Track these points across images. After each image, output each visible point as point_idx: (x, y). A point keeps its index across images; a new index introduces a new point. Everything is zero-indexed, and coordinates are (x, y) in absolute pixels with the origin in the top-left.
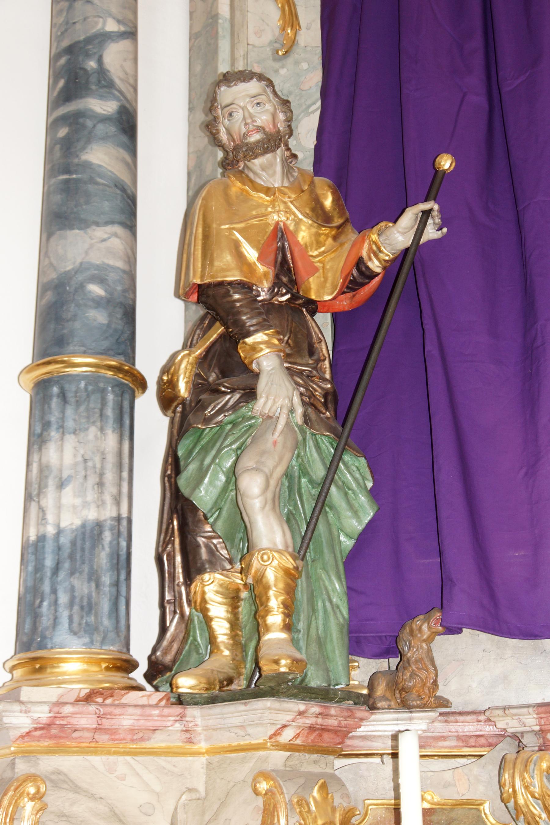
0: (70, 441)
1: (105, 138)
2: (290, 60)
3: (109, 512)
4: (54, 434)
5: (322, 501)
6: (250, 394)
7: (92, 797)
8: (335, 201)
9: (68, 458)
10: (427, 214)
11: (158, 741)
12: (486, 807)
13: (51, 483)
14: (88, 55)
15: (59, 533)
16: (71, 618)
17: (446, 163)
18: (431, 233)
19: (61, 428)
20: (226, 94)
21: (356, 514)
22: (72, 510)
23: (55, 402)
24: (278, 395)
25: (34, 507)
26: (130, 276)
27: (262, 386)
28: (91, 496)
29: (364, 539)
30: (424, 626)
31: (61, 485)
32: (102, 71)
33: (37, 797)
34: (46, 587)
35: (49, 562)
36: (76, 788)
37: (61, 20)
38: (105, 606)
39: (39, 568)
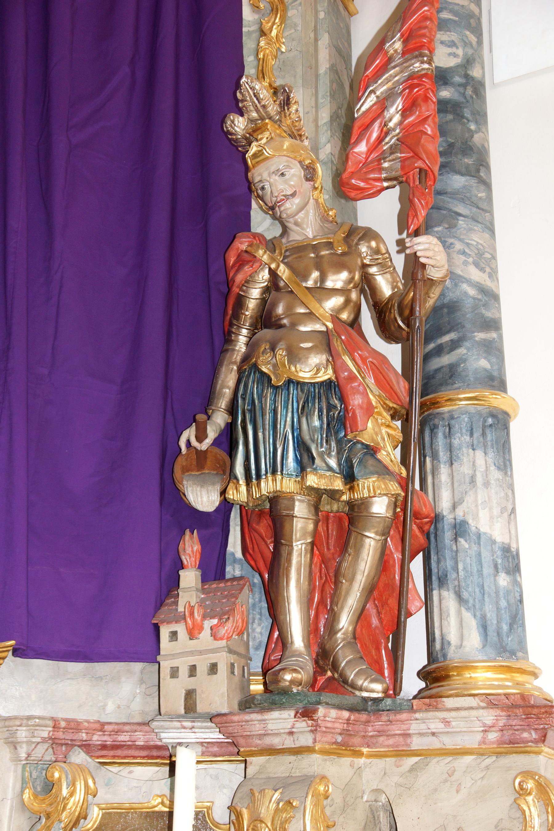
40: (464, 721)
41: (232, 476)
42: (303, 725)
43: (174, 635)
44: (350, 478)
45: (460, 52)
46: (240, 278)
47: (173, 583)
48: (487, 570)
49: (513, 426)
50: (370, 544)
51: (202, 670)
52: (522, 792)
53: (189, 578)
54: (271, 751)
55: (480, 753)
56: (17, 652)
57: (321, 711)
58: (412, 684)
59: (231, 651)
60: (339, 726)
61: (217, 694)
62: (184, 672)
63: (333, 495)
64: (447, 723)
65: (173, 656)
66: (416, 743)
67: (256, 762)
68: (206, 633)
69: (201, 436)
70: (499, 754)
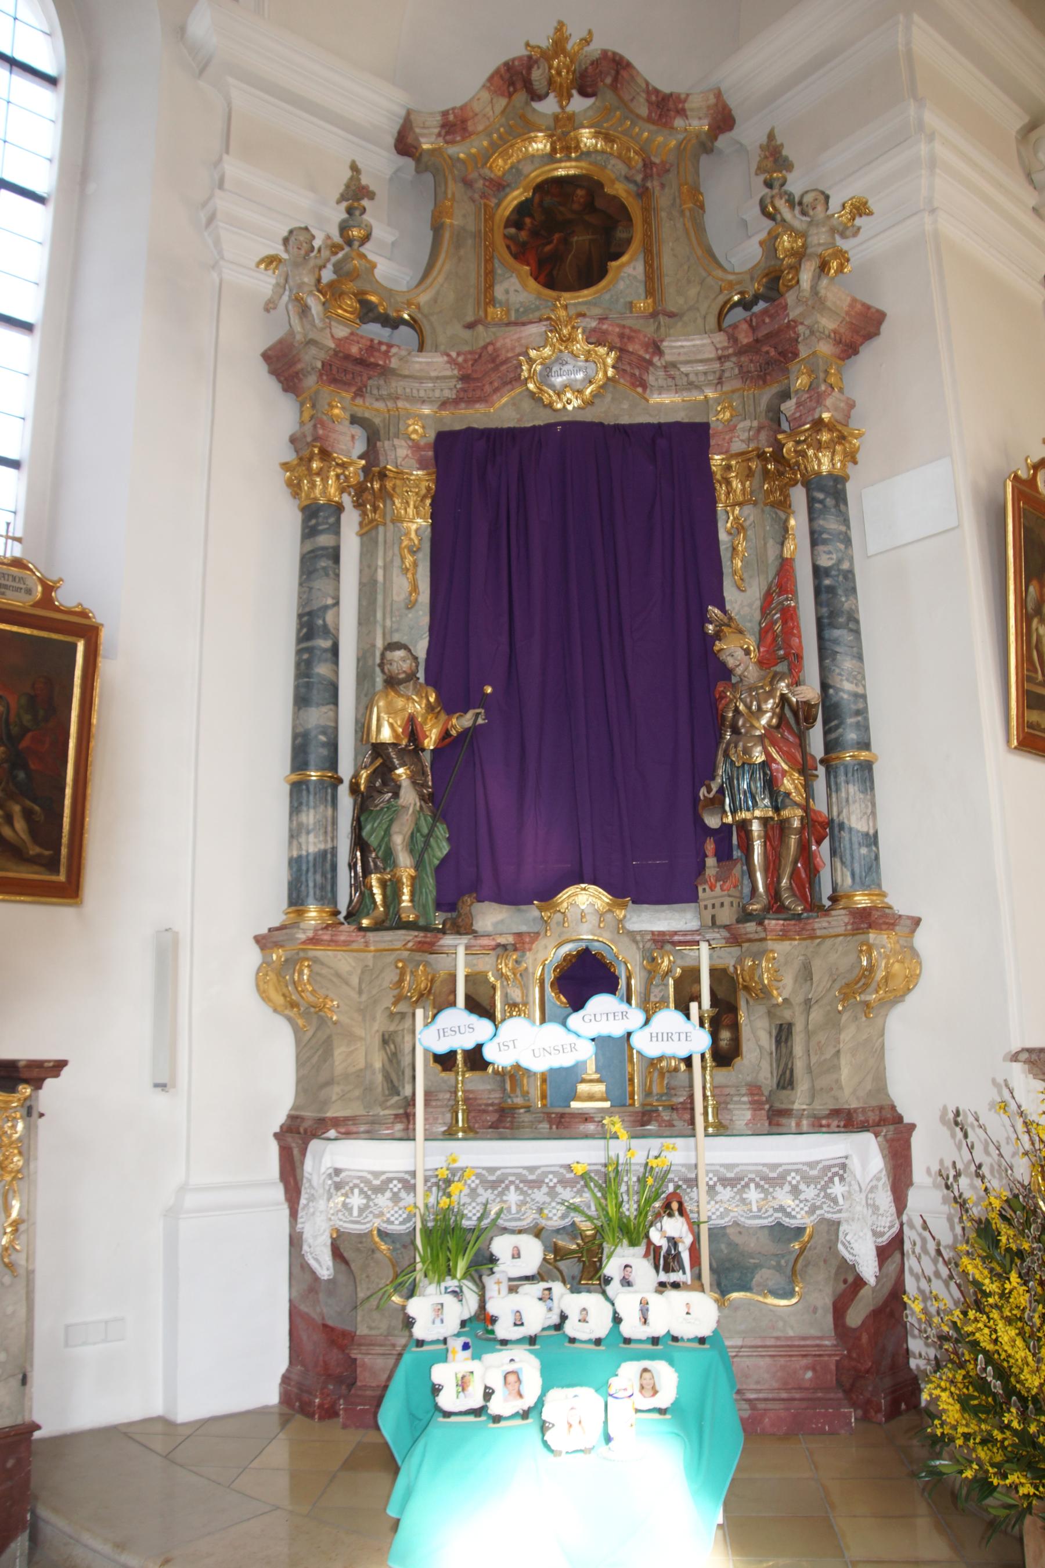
0: (312, 812)
1: (326, 660)
2: (413, 611)
3: (329, 845)
4: (304, 808)
5: (427, 844)
6: (396, 795)
7: (329, 967)
8: (436, 699)
9: (311, 820)
10: (478, 714)
11: (354, 946)
12: (490, 974)
13: (304, 831)
14: (319, 617)
15: (307, 855)
16: (315, 894)
17: (489, 690)
18: (480, 721)
19: (308, 805)
20: (389, 655)
21: (440, 849)
22: (313, 844)
23: (304, 793)
24: (409, 797)
25: (295, 843)
26: (336, 729)
27: (402, 792)
28: (321, 838)
29: (444, 861)
30: (467, 899)
31: (308, 833)
32: (325, 625)
33: (309, 966)
34: (303, 879)
35: (304, 868)
36: (322, 964)
37: (305, 596)
38: (329, 888)
39: (299, 870)
40: (839, 920)
41: (724, 812)
42: (759, 928)
43: (704, 890)
44: (777, 809)
45: (834, 556)
46: (720, 707)
47: (702, 867)
48: (856, 846)
49: (875, 767)
50: (793, 840)
51: (718, 905)
52: (861, 951)
53: (711, 861)
54: (750, 940)
55: (845, 935)
56: (634, 902)
57: (766, 922)
58: (827, 903)
59: (729, 896)
60: (778, 928)
61: (726, 916)
62: (710, 907)
63: (772, 818)
64: (829, 923)
65: (704, 900)
66: (819, 933)
67: (745, 945)
68: (718, 888)
69: (709, 791)
70: (853, 935)
